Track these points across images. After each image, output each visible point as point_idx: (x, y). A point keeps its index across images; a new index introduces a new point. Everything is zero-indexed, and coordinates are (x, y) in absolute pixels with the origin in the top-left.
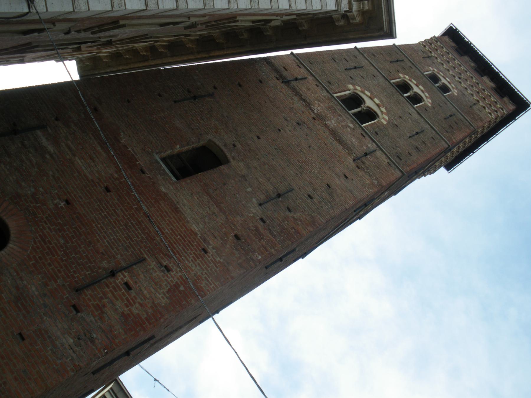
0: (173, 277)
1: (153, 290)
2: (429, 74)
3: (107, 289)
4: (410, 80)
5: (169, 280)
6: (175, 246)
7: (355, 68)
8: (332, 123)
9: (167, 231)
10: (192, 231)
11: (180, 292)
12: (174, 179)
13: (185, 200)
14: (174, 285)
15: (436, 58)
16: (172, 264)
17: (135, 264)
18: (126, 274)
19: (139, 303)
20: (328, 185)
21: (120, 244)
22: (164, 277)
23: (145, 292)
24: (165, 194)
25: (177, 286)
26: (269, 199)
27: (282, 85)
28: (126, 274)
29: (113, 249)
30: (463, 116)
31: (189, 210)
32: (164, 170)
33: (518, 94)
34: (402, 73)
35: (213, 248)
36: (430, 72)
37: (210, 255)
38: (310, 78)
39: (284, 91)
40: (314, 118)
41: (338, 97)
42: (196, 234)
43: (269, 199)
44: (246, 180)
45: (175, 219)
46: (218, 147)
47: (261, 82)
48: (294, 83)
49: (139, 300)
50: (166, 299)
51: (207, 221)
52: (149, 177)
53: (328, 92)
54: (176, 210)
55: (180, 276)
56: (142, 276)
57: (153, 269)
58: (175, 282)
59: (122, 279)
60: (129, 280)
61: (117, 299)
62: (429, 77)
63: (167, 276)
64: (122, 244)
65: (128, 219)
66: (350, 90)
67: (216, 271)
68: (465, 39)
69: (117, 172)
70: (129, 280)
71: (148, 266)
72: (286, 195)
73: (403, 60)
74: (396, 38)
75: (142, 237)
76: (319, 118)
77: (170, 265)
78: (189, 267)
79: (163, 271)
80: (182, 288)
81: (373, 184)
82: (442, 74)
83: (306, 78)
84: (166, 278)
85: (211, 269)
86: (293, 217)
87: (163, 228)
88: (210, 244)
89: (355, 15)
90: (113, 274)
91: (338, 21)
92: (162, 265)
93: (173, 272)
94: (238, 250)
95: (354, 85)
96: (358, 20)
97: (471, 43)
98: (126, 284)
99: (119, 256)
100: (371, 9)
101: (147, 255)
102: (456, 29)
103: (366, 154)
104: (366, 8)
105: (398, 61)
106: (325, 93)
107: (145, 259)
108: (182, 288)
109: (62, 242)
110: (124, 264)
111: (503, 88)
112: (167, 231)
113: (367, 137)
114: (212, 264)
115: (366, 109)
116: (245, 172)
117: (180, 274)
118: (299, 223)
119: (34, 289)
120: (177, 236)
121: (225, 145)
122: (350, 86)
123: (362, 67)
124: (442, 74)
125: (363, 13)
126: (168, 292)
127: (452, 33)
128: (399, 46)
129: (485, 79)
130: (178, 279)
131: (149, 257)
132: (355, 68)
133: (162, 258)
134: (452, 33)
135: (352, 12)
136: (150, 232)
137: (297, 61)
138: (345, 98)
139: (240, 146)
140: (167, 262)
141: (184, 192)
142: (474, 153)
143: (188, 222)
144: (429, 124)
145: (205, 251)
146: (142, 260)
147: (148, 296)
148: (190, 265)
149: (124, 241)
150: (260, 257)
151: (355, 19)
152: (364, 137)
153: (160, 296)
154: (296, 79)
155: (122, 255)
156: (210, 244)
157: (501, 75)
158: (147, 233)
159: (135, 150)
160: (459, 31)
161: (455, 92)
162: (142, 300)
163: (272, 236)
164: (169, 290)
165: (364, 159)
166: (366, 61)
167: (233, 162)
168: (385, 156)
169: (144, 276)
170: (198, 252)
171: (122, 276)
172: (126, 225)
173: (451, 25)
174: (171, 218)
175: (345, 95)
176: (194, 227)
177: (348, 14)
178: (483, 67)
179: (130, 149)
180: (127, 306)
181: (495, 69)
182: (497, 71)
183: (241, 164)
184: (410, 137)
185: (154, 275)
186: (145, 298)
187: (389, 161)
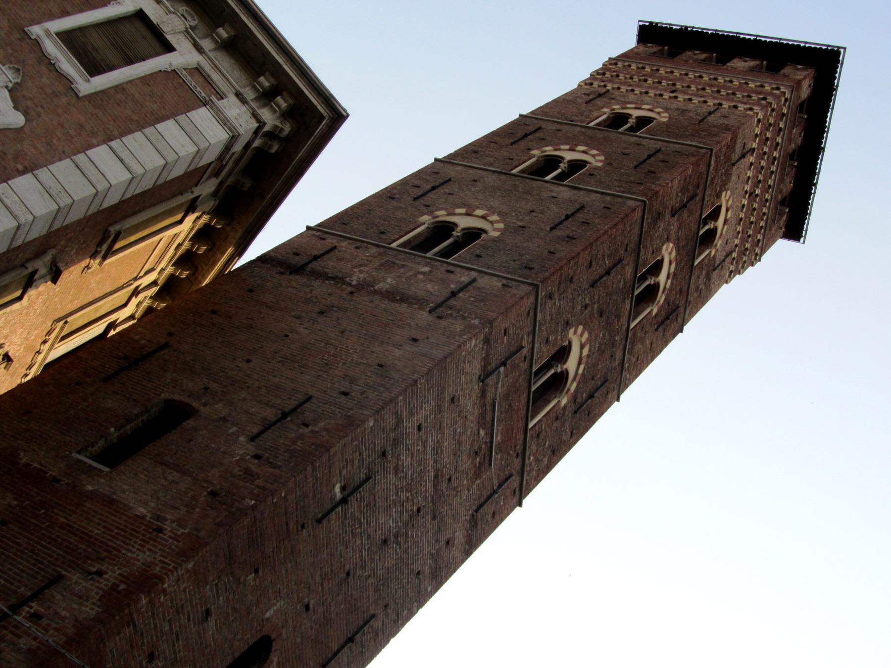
0: (107, 580)
1: (75, 606)
2: (604, 121)
3: (5, 632)
4: (556, 150)
5: (102, 585)
6: (110, 543)
7: (433, 188)
8: (389, 281)
9: (96, 531)
10: (136, 515)
11: (119, 592)
12: (107, 469)
14: (111, 588)
15: (619, 88)
16: (106, 565)
17: (47, 587)
18: (33, 604)
19: (56, 630)
20: (380, 365)
21: (24, 575)
22: (92, 585)
23: (63, 613)
24: (92, 492)
25: (114, 587)
27: (292, 277)
28: (33, 604)
29: (13, 584)
30: (679, 144)
31: (131, 495)
32: (90, 466)
33: (810, 47)
34: (537, 149)
35: (173, 522)
36: (604, 117)
37: (167, 532)
38: (344, 244)
39: (294, 284)
40: (352, 293)
41: (403, 245)
42: (143, 517)
45: (110, 513)
46: (180, 402)
47: (251, 291)
48: (314, 265)
49: (54, 625)
50: (97, 609)
51: (161, 494)
52: (67, 484)
53: (378, 246)
54: (110, 502)
55: (120, 574)
56: (59, 597)
57: (76, 582)
58: (110, 584)
59: (28, 612)
60: (39, 608)
62: (608, 126)
63: (98, 582)
64: (28, 574)
65: (36, 542)
66: (424, 223)
67: (177, 546)
68: (674, 27)
69: (15, 499)
70: (39, 608)
71: (69, 583)
72: (299, 410)
73: (540, 128)
74: (338, 117)
75: (59, 555)
76: (363, 287)
77: (103, 568)
78: (133, 559)
79: (91, 579)
81: (470, 327)
82: (633, 106)
83: (335, 248)
84: (97, 584)
85: (169, 548)
86: (313, 432)
87: (91, 531)
88: (166, 520)
89: (279, 124)
91: (271, 147)
92: (90, 573)
93: (106, 573)
95: (430, 213)
96: (287, 128)
97: (687, 28)
99: (23, 589)
100: (291, 102)
101: (66, 570)
102: (651, 23)
103: (454, 294)
104: (284, 105)
105: (526, 135)
106: (373, 250)
107: (60, 577)
108: (122, 587)
111: (774, 56)
112: (96, 531)
113: (458, 269)
114: (171, 541)
115: (463, 234)
116: (225, 412)
117: (118, 572)
120: (112, 531)
121: (190, 395)
122: (426, 218)
123: (450, 180)
124: (633, 106)
125: (286, 115)
126: (99, 600)
127: (650, 33)
128: (533, 112)
129: (738, 64)
130: (116, 578)
131: (69, 572)
132: (433, 188)
133: (91, 565)
134: (650, 33)
135: (264, 124)
136: (71, 543)
137: (318, 234)
138: (422, 239)
139: (215, 385)
140: (98, 566)
141: (124, 477)
142: (815, 185)
143: (131, 508)
144: (597, 192)
145: (160, 530)
146: (58, 579)
147: (68, 615)
148: (134, 556)
149: (31, 569)
150: (253, 502)
151: (282, 130)
152: (452, 272)
153: (87, 609)
154: (315, 258)
155: (26, 586)
156: (166, 520)
157: (763, 39)
158: (67, 547)
159: (43, 462)
160: (657, 24)
161: (664, 118)
162: (58, 623)
163: (275, 468)
164: (102, 596)
165: (452, 302)
166: (459, 168)
167: (203, 409)
168: (495, 278)
169: (63, 595)
170: (148, 536)
171: (28, 609)
172: (32, 551)
173: (641, 24)
174: (103, 515)
175: (419, 234)
176: (142, 510)
177: (267, 128)
178: (721, 47)
179: (35, 465)
181: (747, 37)
182: (752, 38)
183: (219, 406)
184: (551, 229)
185: (77, 588)
186: (63, 619)
187: (505, 281)
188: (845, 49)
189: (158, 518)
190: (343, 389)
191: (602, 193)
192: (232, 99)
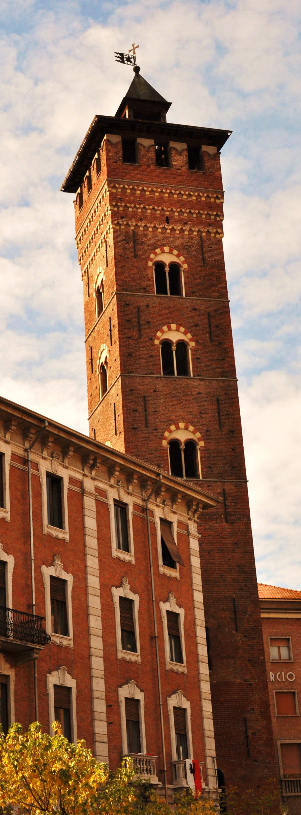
13: (224, 675)
19: (262, 734)
23: (259, 728)
26: (235, 620)
28: (249, 731)
35: (251, 679)
42: (241, 682)
43: (235, 620)
44: (221, 626)
61: (257, 742)
80: (263, 710)
86: (250, 615)
90: (247, 737)
94: (255, 667)
98: (253, 733)
108: (263, 710)
109: (227, 749)
110: (244, 729)
118: (253, 614)
119: (242, 772)
144: (214, 380)
145: (251, 684)
146: (245, 719)
176: (238, 681)
180: (261, 740)
188: (231, 132)
189: (246, 680)
190: (239, 587)
191: (216, 380)
192: (189, 522)
